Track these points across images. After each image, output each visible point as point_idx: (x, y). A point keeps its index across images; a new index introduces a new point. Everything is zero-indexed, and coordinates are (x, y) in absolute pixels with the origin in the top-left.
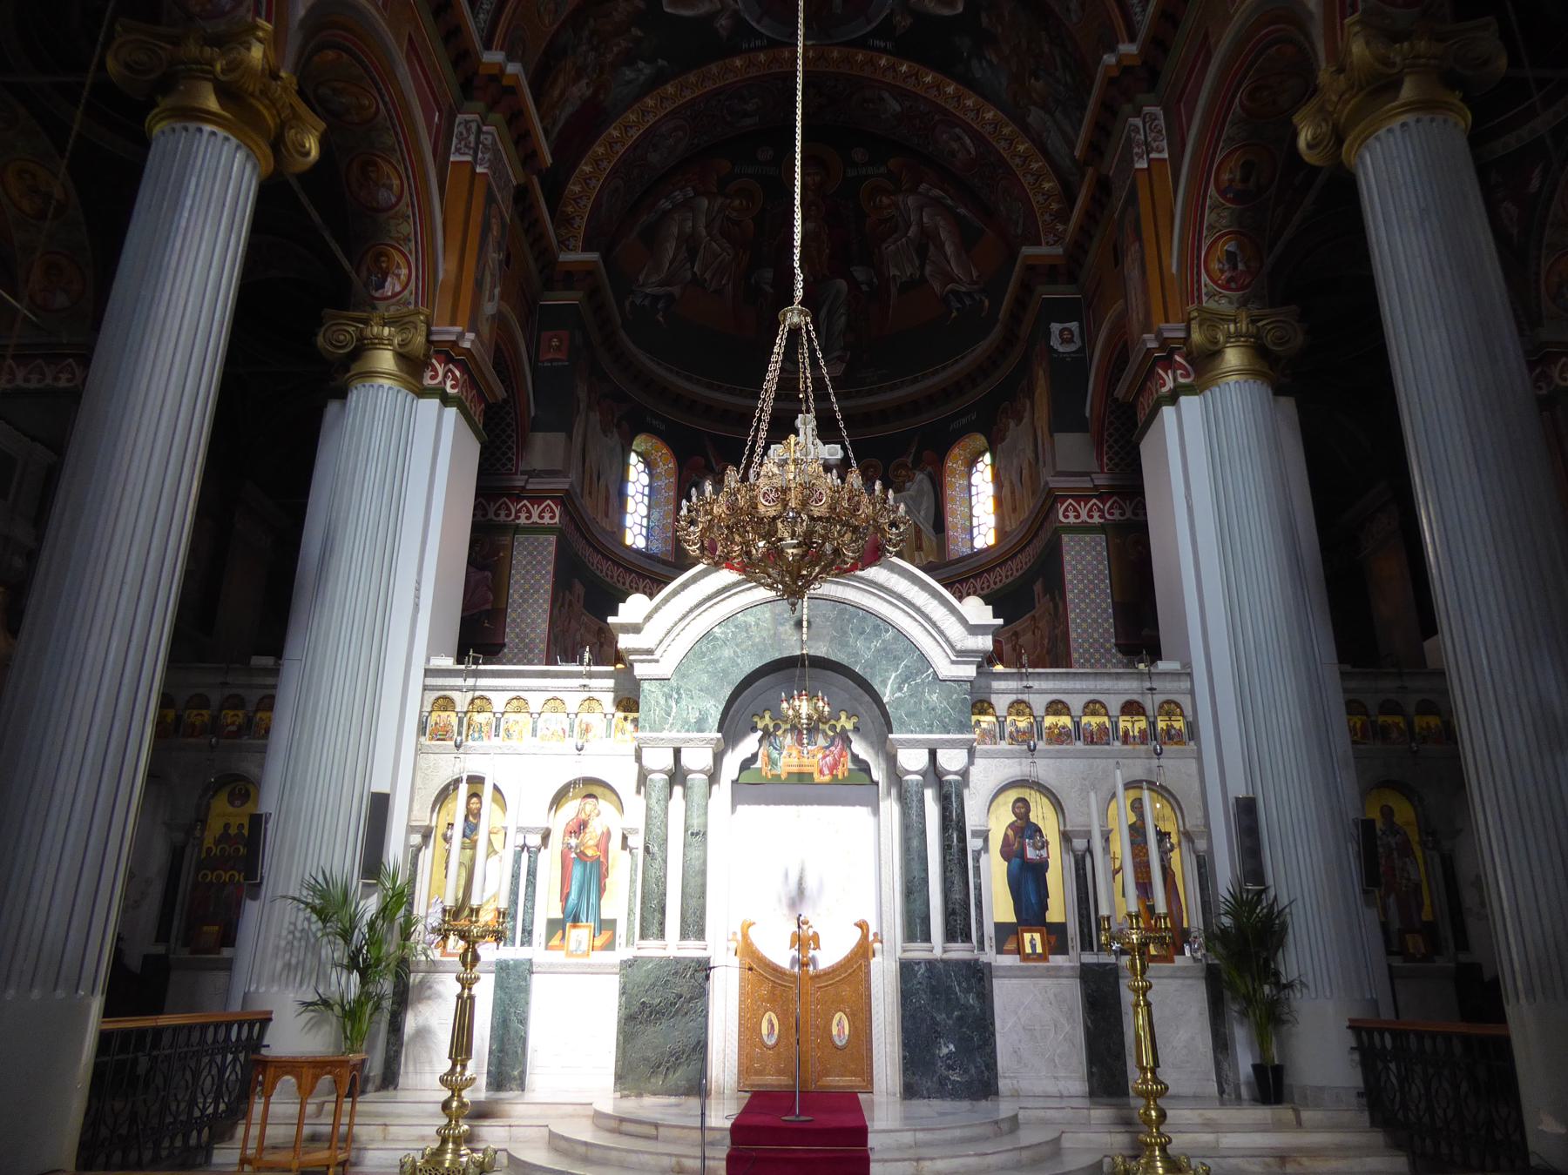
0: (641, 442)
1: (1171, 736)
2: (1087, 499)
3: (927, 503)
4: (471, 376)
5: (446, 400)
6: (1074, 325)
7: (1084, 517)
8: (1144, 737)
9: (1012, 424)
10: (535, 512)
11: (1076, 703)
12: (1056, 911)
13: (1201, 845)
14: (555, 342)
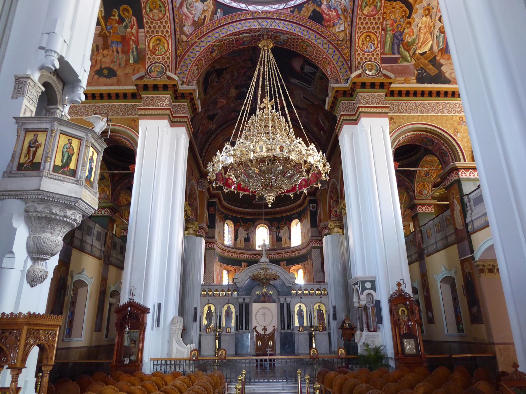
0: (227, 221)
1: (325, 294)
2: (317, 241)
3: (287, 233)
4: (204, 231)
5: (201, 236)
6: (315, 205)
7: (316, 245)
8: (321, 294)
9: (304, 219)
10: (210, 245)
11: (309, 289)
12: (305, 324)
13: (328, 313)
14: (212, 209)
